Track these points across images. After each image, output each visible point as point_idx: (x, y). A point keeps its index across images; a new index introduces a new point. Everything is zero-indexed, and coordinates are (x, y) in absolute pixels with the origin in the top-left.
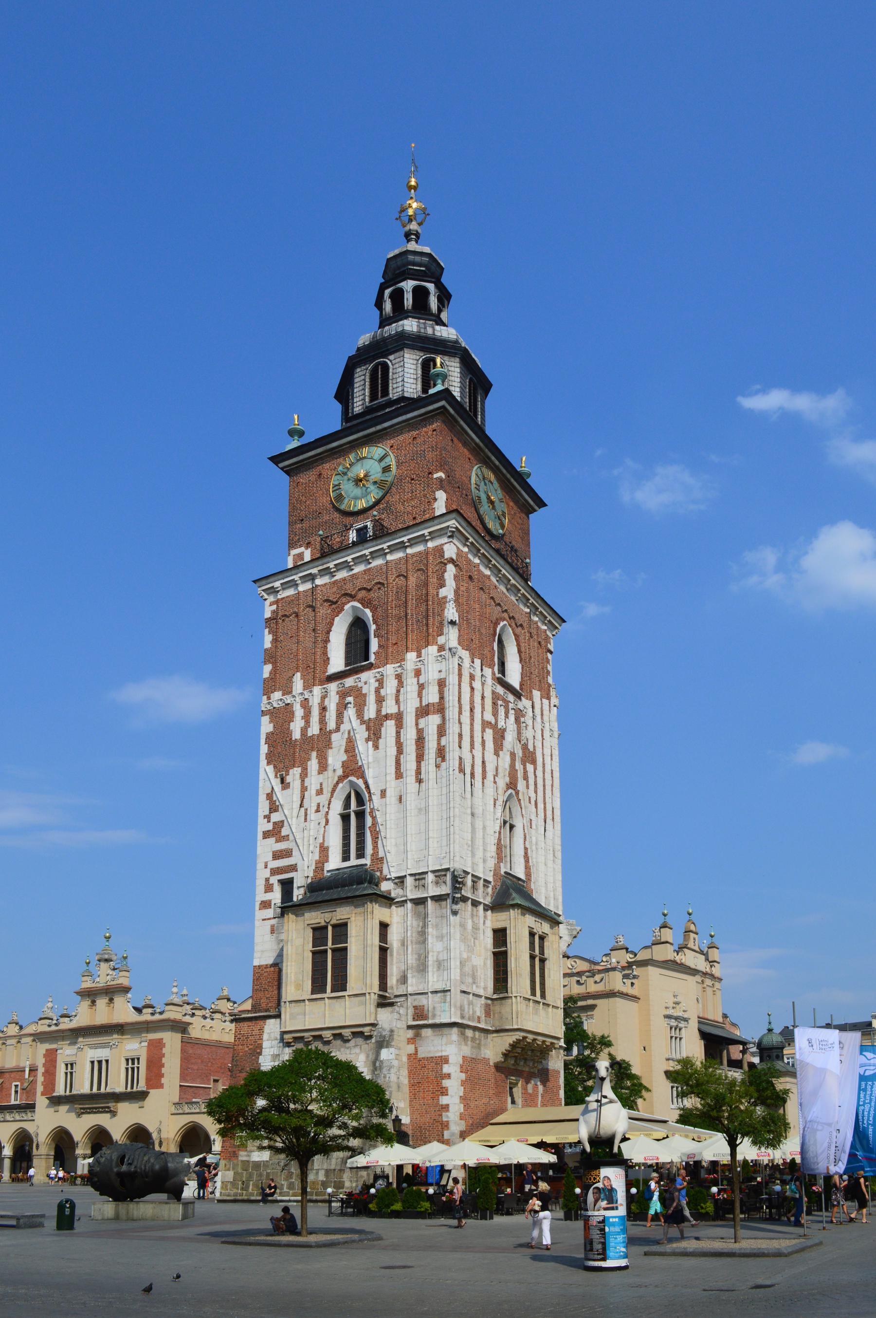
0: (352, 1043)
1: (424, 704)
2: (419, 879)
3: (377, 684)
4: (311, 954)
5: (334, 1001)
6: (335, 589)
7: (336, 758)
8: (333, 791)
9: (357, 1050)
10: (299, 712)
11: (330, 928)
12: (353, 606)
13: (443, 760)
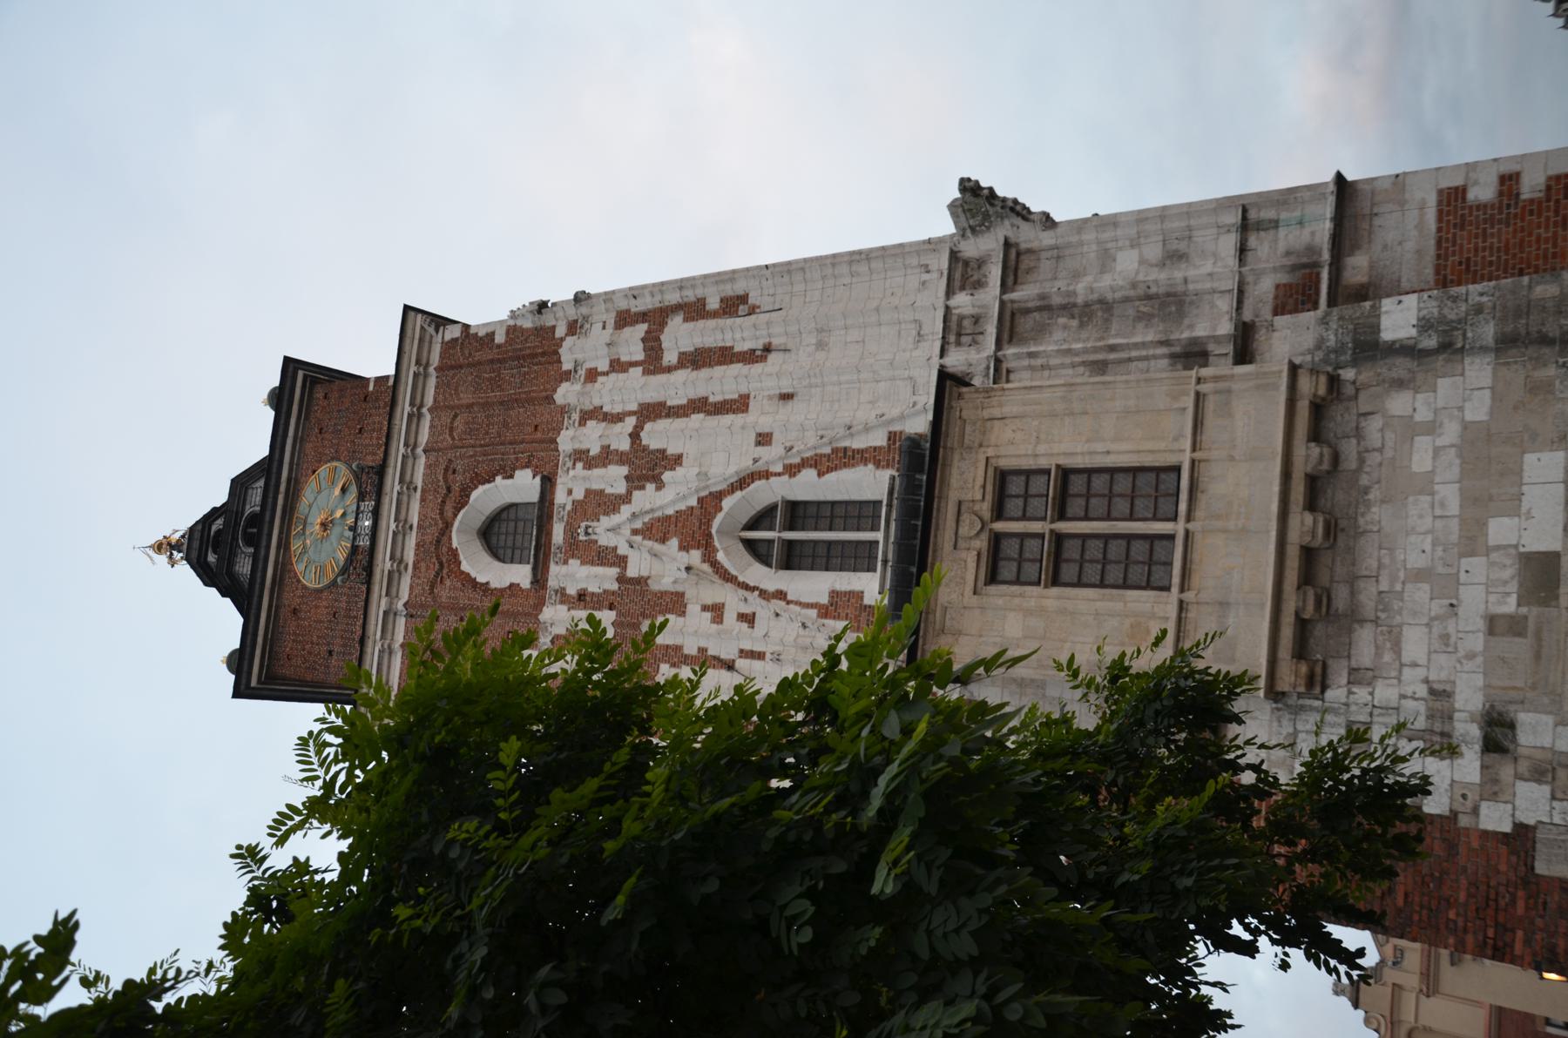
0: (1349, 449)
1: (640, 356)
2: (959, 335)
3: (580, 465)
4: (1055, 591)
5: (1203, 500)
6: (423, 565)
7: (665, 566)
8: (727, 577)
9: (1373, 426)
11: (1000, 526)
12: (458, 531)
13: (743, 299)
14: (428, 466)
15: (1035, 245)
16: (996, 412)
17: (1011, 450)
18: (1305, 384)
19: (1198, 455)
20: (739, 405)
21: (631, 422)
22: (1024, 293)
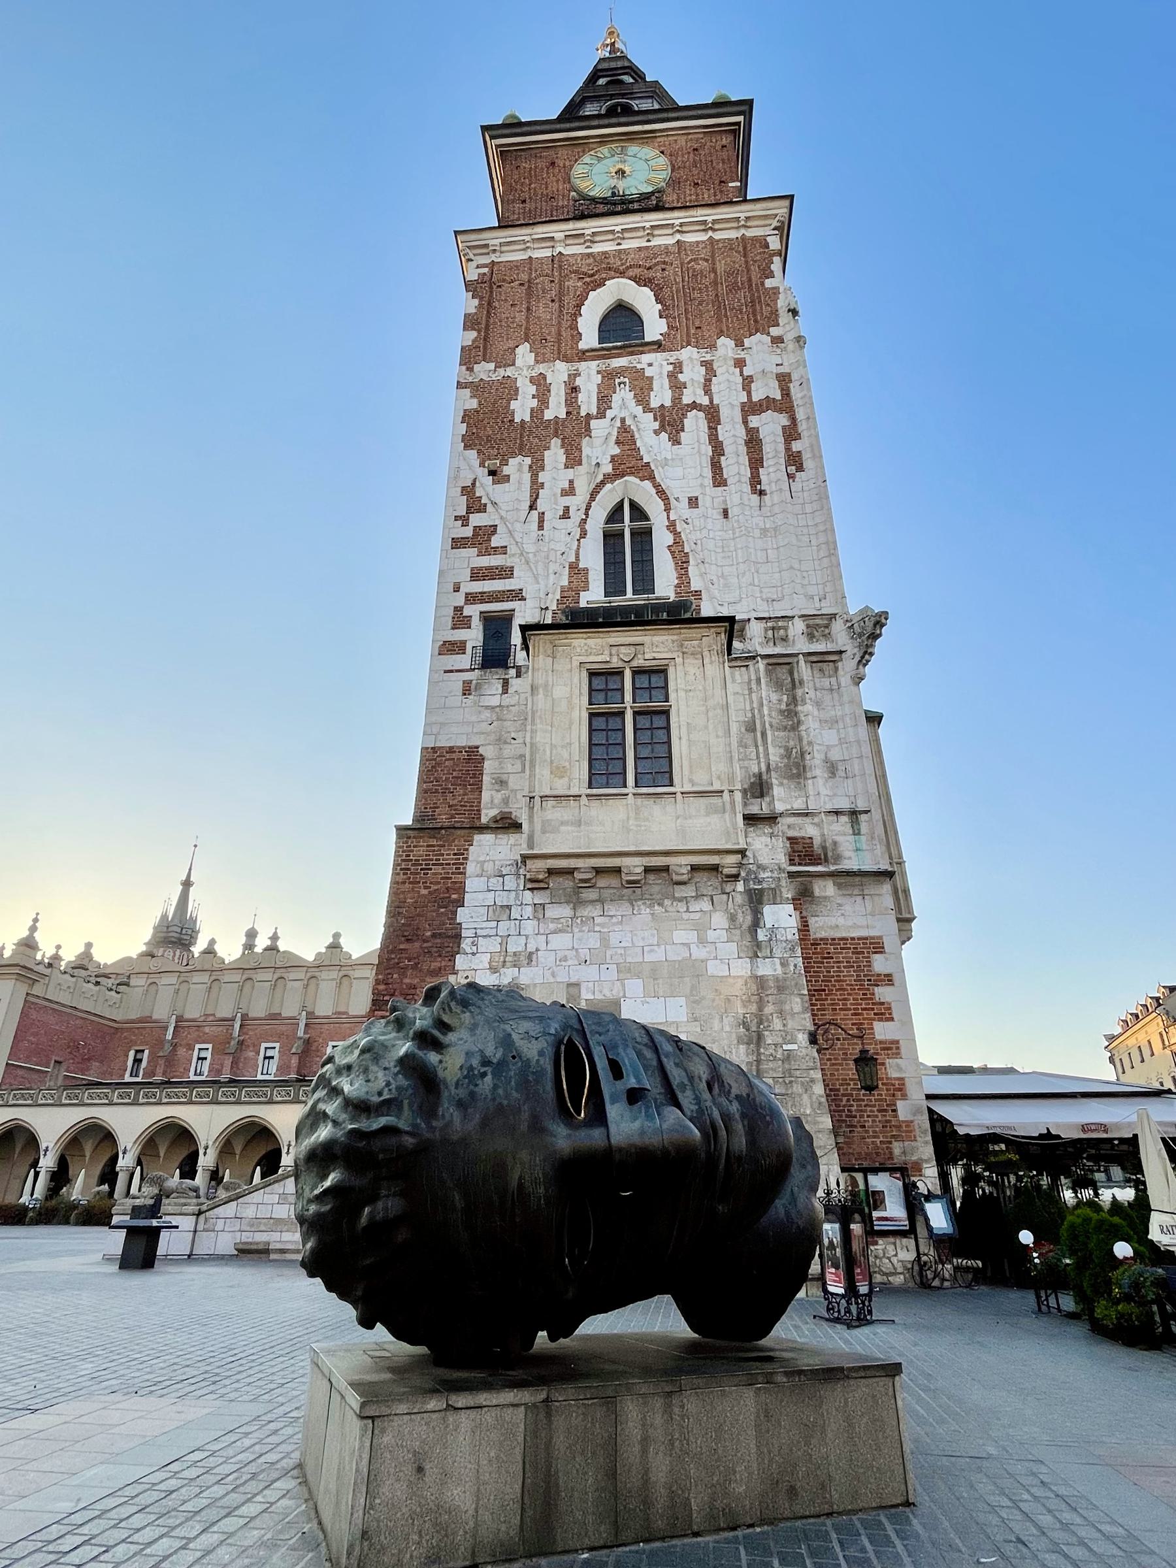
0: (688, 891)
1: (755, 399)
2: (773, 629)
4: (585, 715)
7: (600, 448)
8: (593, 495)
9: (705, 905)
10: (527, 390)
13: (800, 468)
14: (666, 247)
15: (841, 672)
16: (706, 661)
17: (680, 674)
18: (733, 859)
19: (679, 796)
20: (719, 480)
21: (705, 401)
22: (804, 669)
